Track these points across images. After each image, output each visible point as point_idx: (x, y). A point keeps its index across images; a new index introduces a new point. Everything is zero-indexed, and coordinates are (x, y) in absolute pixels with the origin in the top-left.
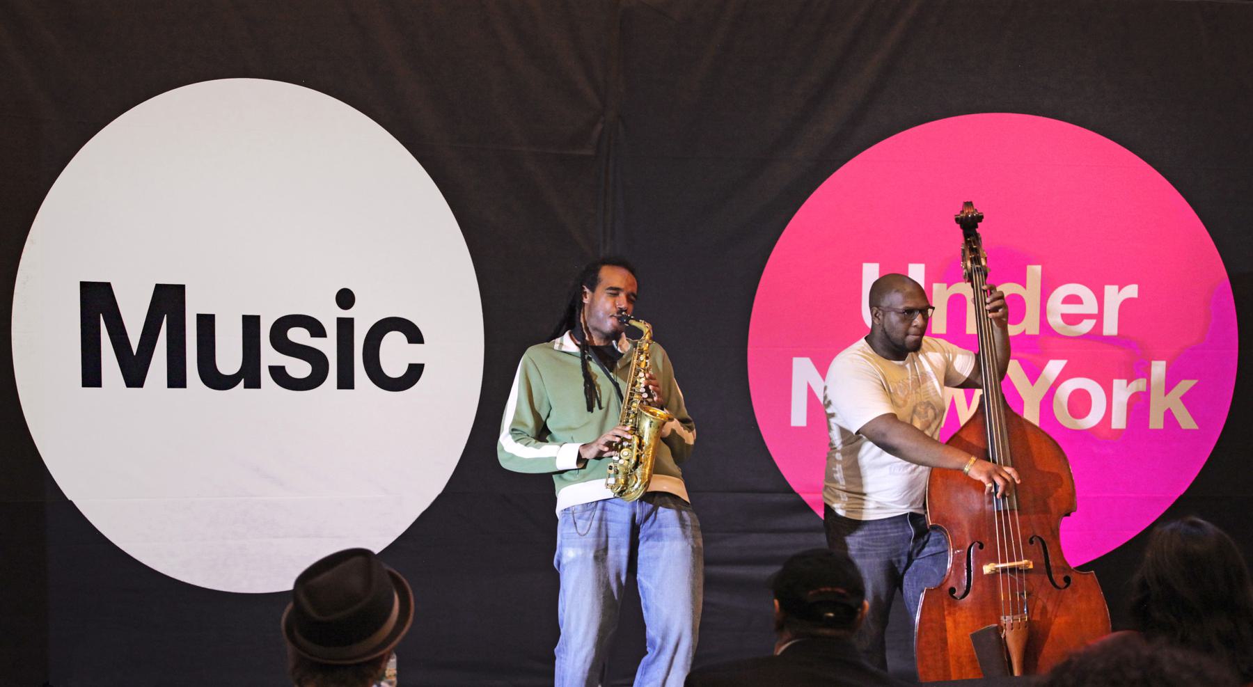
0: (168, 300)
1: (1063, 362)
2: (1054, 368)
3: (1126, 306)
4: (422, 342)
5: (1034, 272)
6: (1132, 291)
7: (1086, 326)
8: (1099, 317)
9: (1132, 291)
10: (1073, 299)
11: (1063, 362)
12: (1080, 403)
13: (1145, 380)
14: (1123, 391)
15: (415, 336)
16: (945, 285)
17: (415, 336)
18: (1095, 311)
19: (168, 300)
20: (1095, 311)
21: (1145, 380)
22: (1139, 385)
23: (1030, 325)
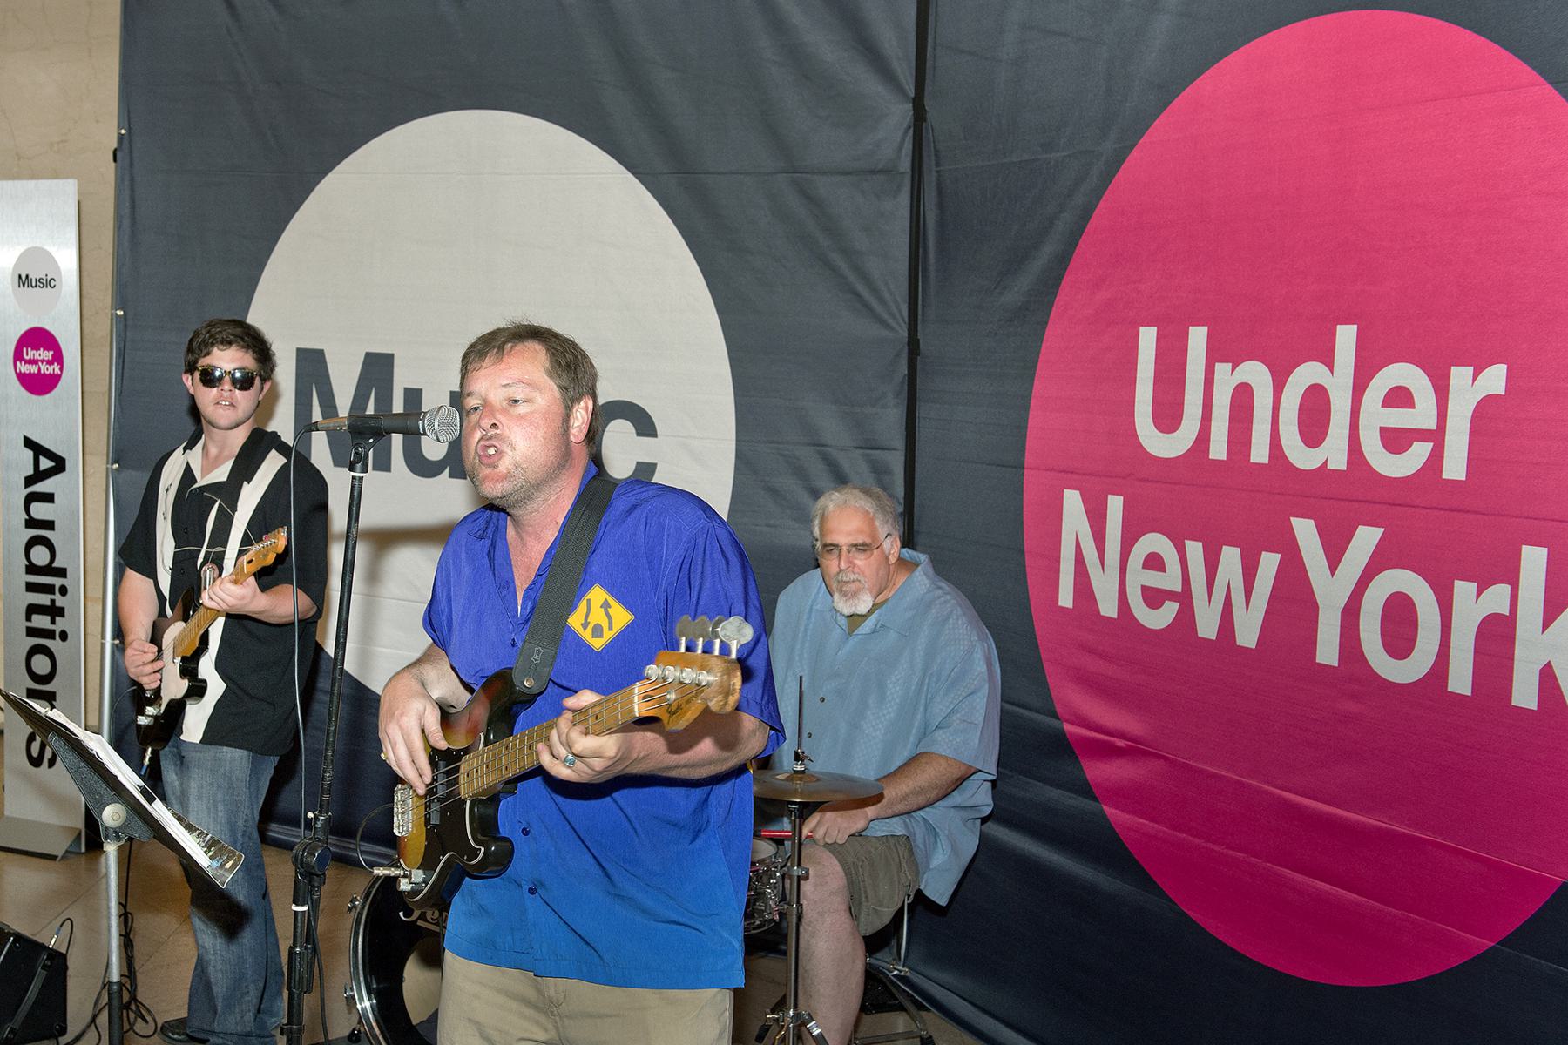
0: (378, 368)
1: (1378, 532)
2: (1366, 539)
3: (1486, 410)
4: (655, 436)
5: (1346, 337)
6: (1495, 379)
7: (1419, 453)
8: (1436, 436)
9: (1495, 379)
10: (1399, 397)
11: (1378, 532)
12: (1400, 624)
13: (1503, 590)
14: (1473, 604)
15: (645, 425)
16: (1229, 365)
17: (645, 425)
18: (1431, 424)
19: (378, 368)
20: (1431, 424)
21: (1508, 588)
22: (1496, 599)
23: (1333, 452)
